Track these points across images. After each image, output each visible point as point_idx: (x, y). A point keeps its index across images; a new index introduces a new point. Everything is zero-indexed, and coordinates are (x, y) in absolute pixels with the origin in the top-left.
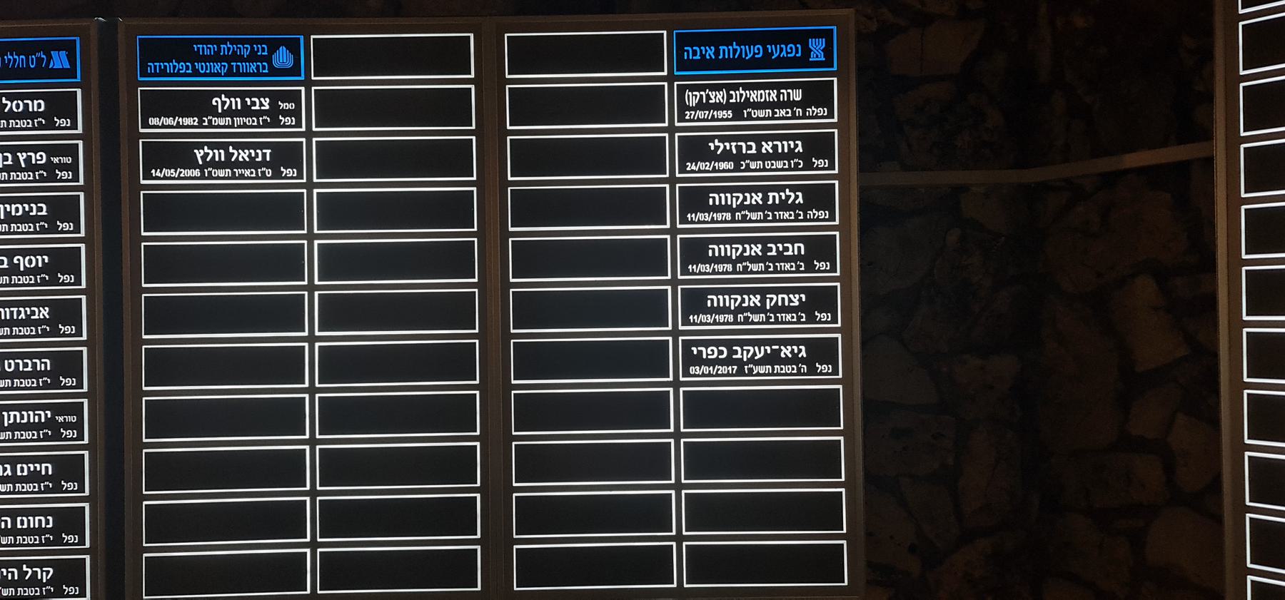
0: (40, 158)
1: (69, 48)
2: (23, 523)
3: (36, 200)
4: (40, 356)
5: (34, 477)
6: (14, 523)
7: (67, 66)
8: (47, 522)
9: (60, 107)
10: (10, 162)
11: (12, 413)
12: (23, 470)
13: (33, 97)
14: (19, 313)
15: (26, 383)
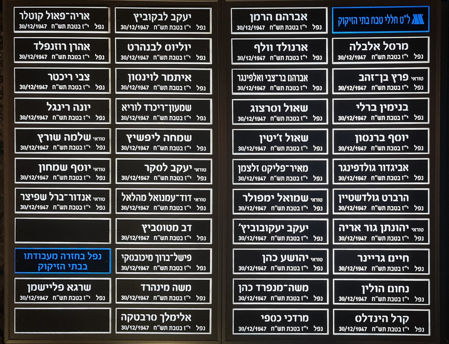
0: (405, 77)
1: (424, 11)
2: (391, 289)
3: (402, 102)
4: (403, 193)
5: (398, 263)
6: (386, 289)
7: (422, 23)
8: (406, 289)
9: (417, 47)
10: (387, 80)
11: (386, 226)
12: (392, 259)
13: (401, 41)
14: (391, 168)
15: (394, 208)
